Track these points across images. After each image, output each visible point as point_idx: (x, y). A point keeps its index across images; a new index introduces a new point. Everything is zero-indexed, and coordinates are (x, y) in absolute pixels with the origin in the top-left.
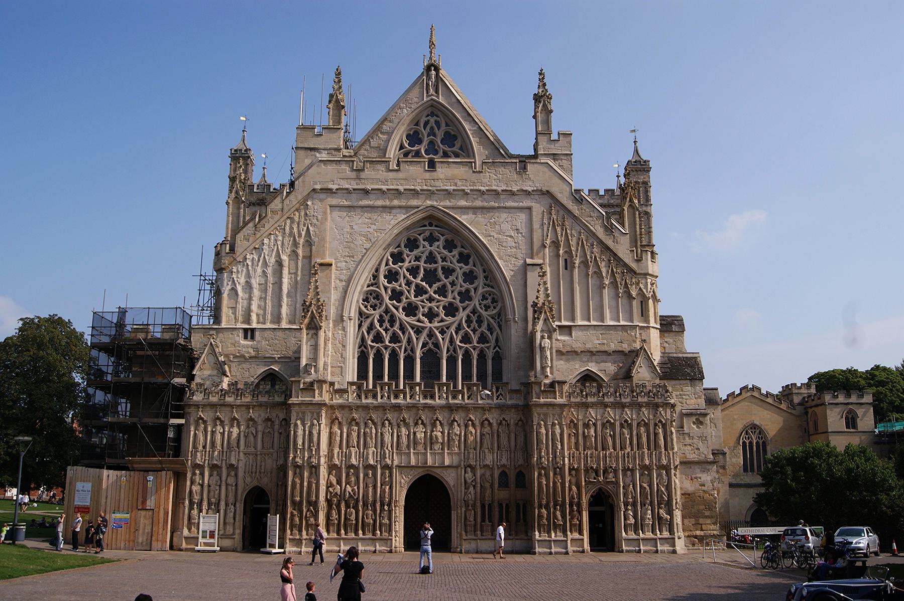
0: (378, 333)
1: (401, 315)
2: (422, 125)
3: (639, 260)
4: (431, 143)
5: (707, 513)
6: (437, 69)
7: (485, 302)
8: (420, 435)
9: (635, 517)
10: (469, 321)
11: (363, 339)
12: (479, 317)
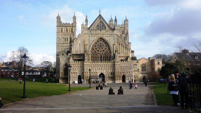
0: (94, 54)
1: (97, 51)
3: (129, 44)
8: (101, 68)
10: (106, 52)
12: (107, 52)
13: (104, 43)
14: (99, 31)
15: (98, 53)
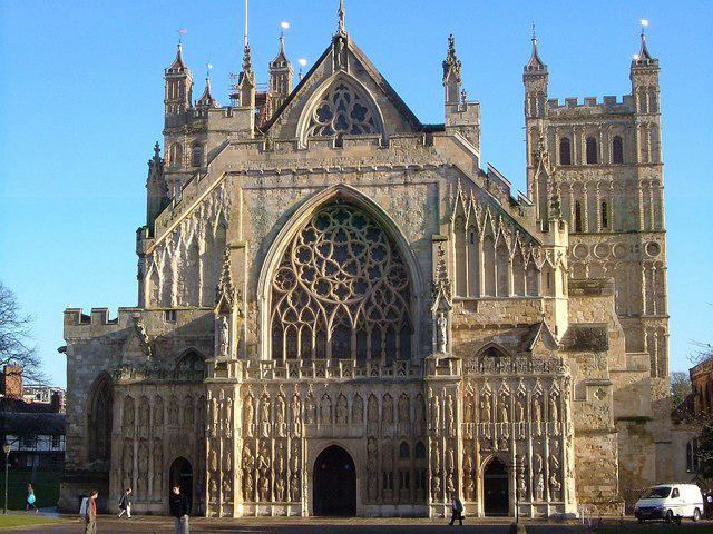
1: (313, 292)
2: (331, 98)
4: (341, 118)
5: (607, 481)
6: (345, 40)
7: (394, 278)
9: (527, 484)
10: (378, 296)
11: (277, 316)
13: (365, 229)
14: (326, 154)
15: (323, 303)
